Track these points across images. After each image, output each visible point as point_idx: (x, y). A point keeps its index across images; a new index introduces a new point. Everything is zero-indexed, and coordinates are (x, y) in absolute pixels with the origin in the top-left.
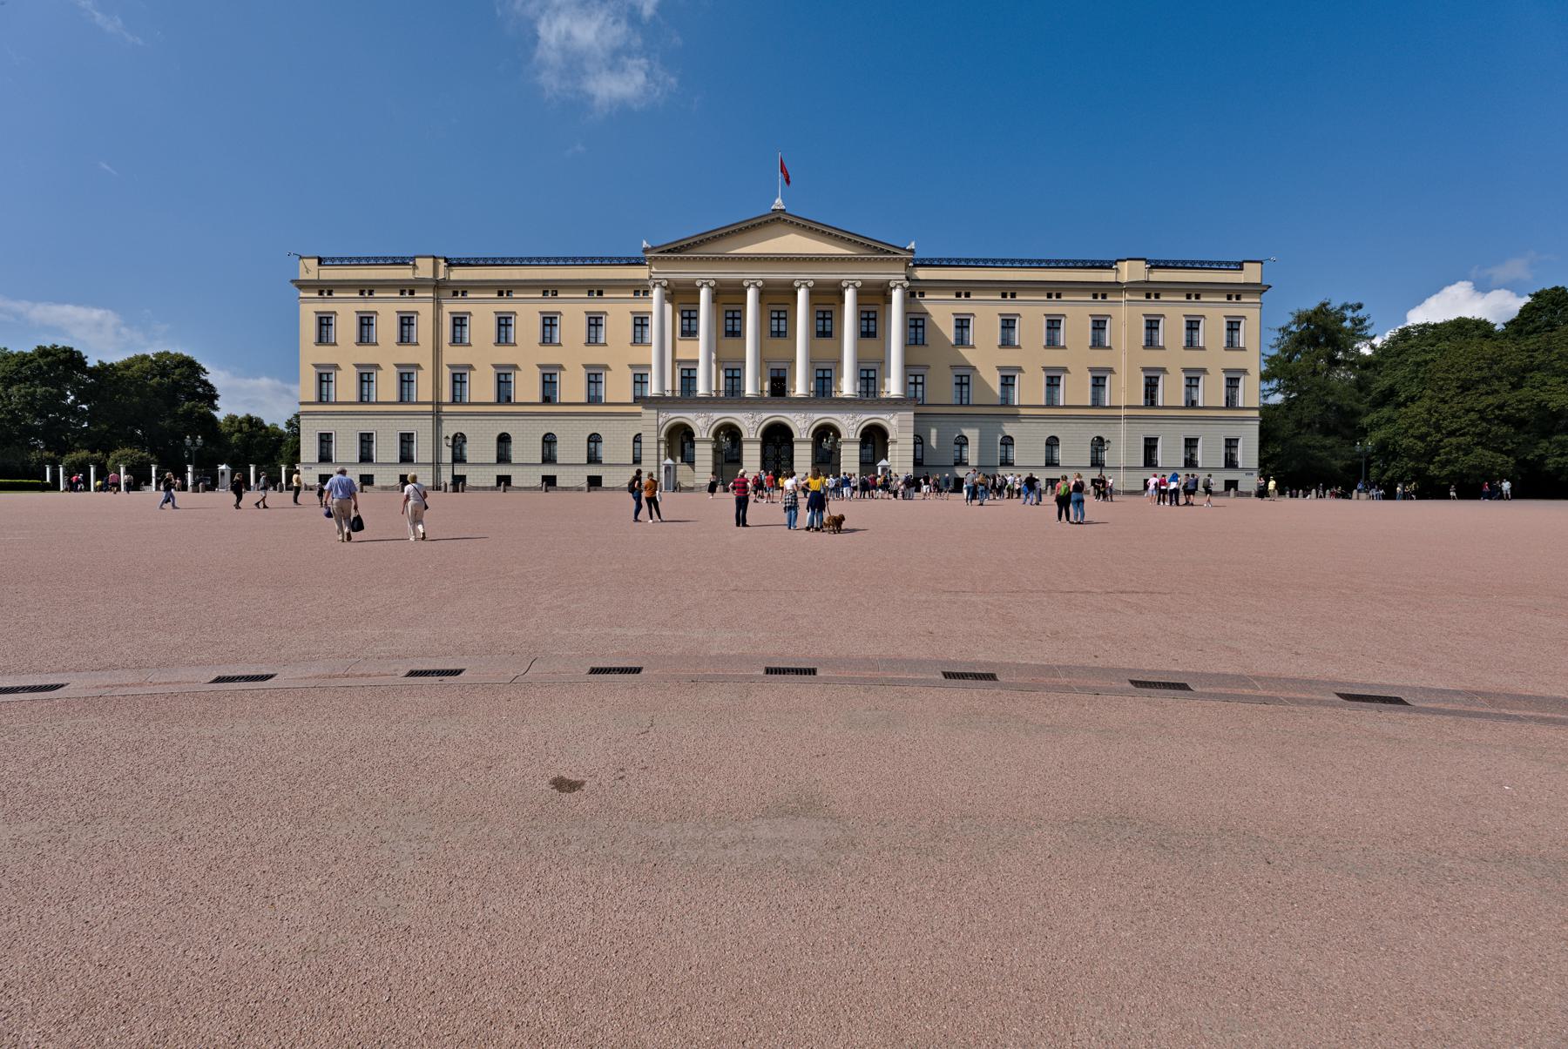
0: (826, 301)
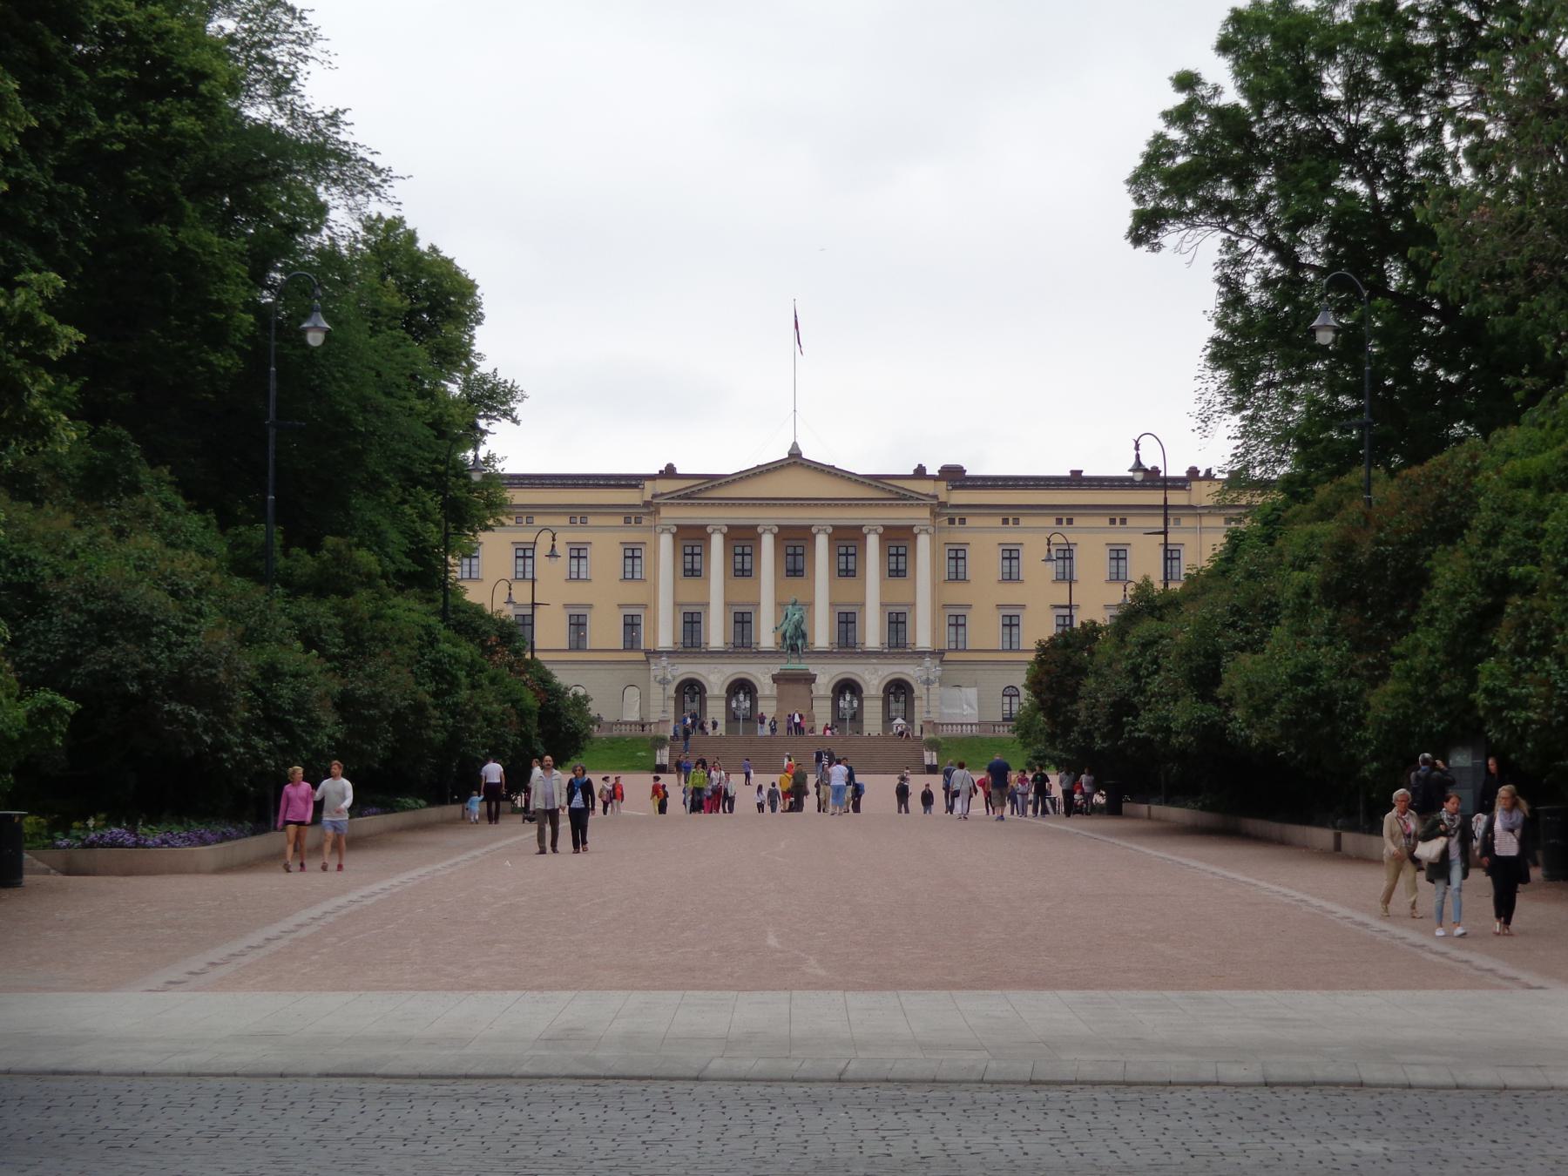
0: (847, 542)
